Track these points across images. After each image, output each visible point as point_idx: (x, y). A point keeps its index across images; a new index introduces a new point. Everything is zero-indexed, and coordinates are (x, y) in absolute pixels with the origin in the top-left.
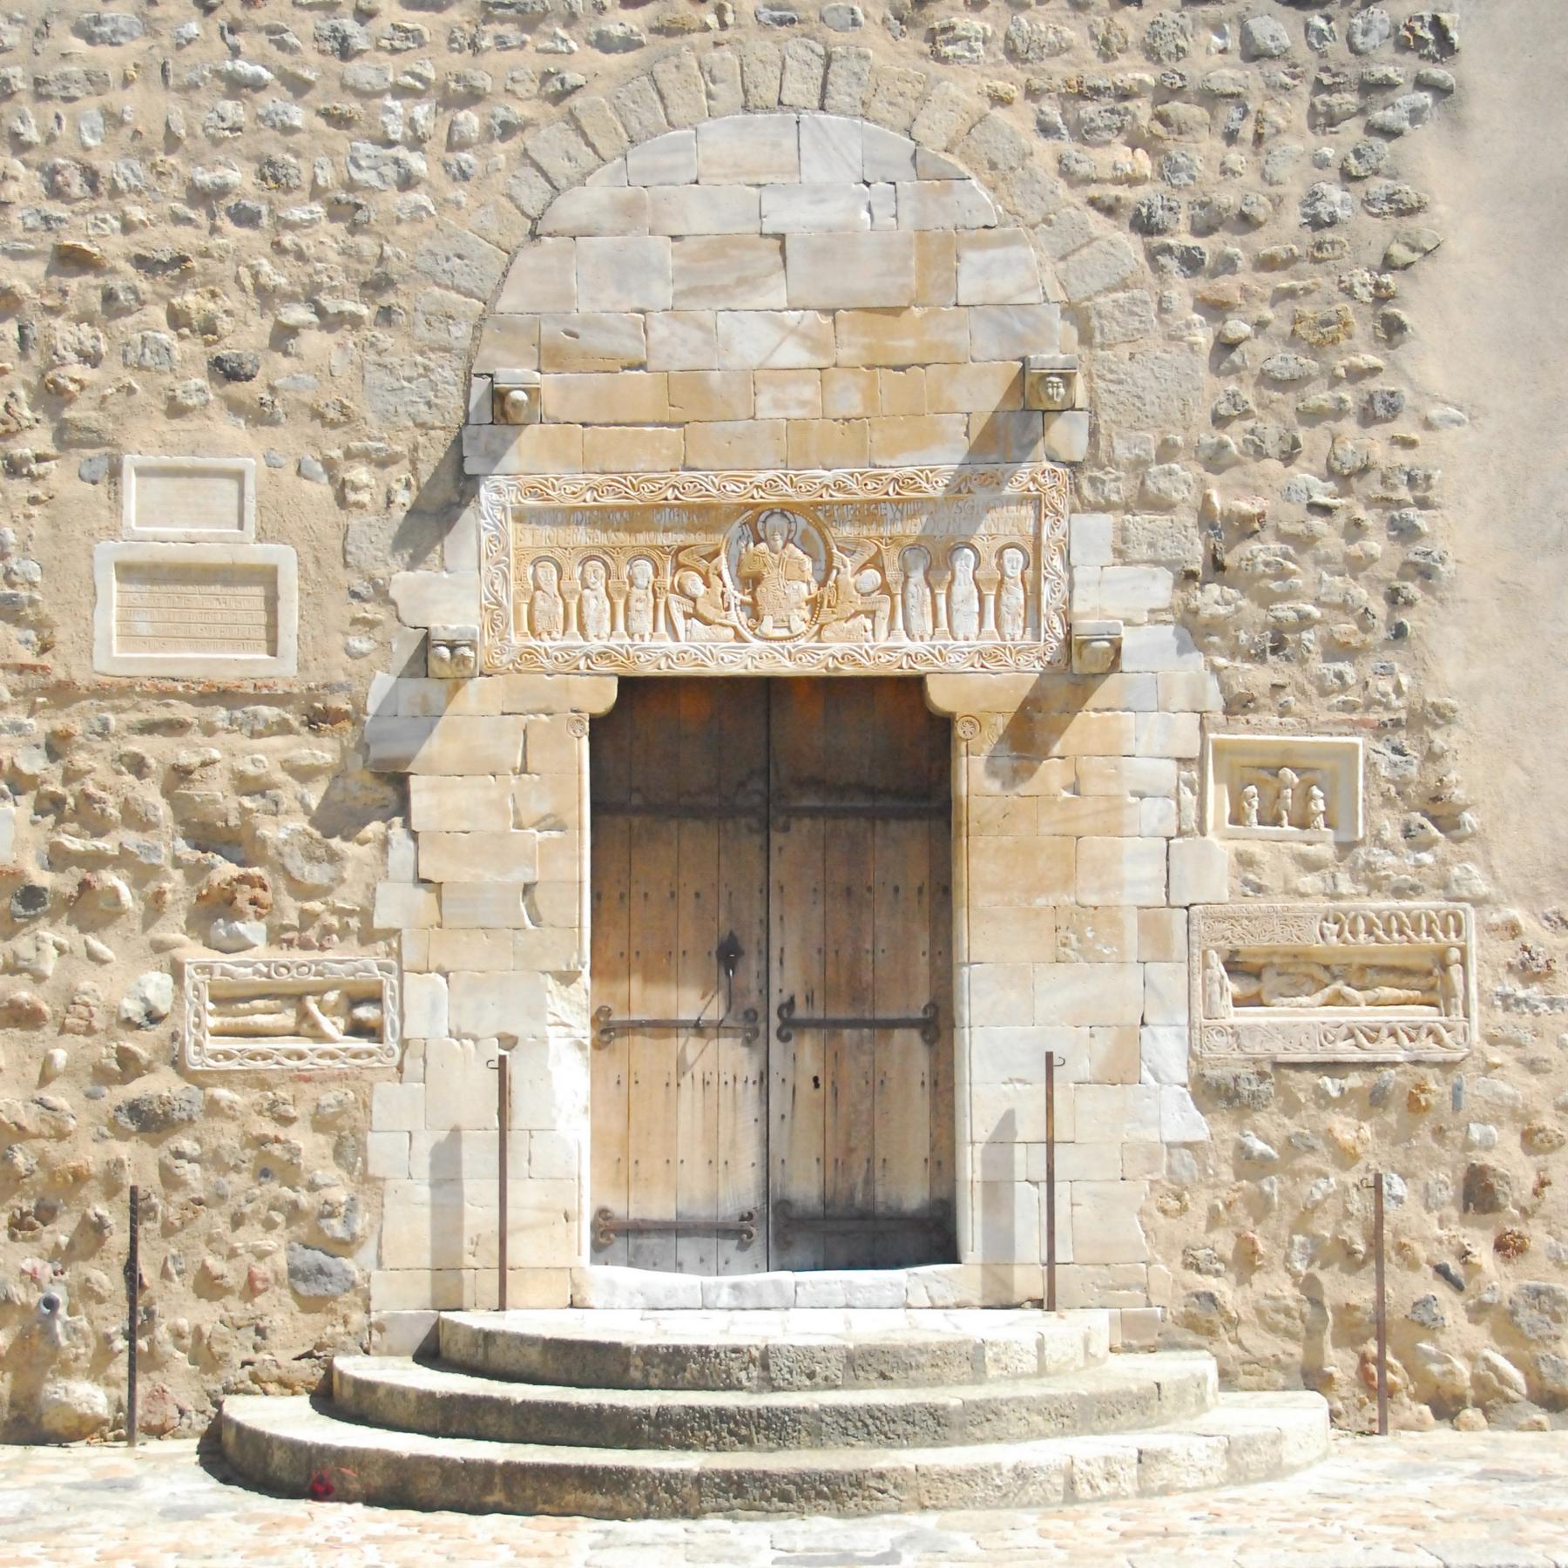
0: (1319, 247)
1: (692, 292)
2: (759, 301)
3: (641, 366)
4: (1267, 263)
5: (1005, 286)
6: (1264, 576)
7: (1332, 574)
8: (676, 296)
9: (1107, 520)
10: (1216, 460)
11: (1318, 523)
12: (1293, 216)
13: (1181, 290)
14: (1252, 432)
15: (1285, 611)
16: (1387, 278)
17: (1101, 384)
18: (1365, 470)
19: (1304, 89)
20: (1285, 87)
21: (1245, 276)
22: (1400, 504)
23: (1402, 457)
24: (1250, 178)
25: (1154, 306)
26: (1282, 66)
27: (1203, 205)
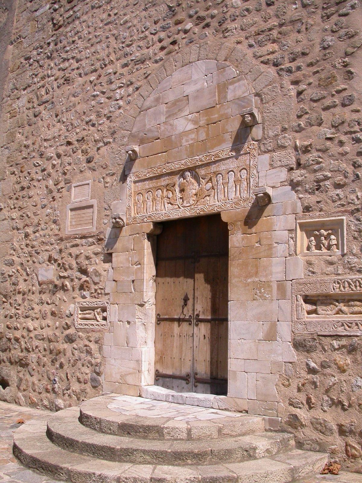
0: (325, 55)
1: (169, 116)
2: (183, 114)
3: (159, 138)
4: (311, 65)
5: (239, 93)
6: (312, 164)
7: (334, 160)
8: (166, 118)
9: (267, 156)
10: (299, 130)
11: (328, 143)
12: (317, 48)
13: (287, 80)
14: (308, 119)
15: (319, 175)
16: (346, 59)
17: (265, 114)
18: (343, 123)
19: (319, 11)
20: (313, 12)
21: (306, 71)
22: (355, 132)
23: (355, 116)
24: (305, 42)
25: (279, 87)
26: (313, 7)
27: (291, 54)
